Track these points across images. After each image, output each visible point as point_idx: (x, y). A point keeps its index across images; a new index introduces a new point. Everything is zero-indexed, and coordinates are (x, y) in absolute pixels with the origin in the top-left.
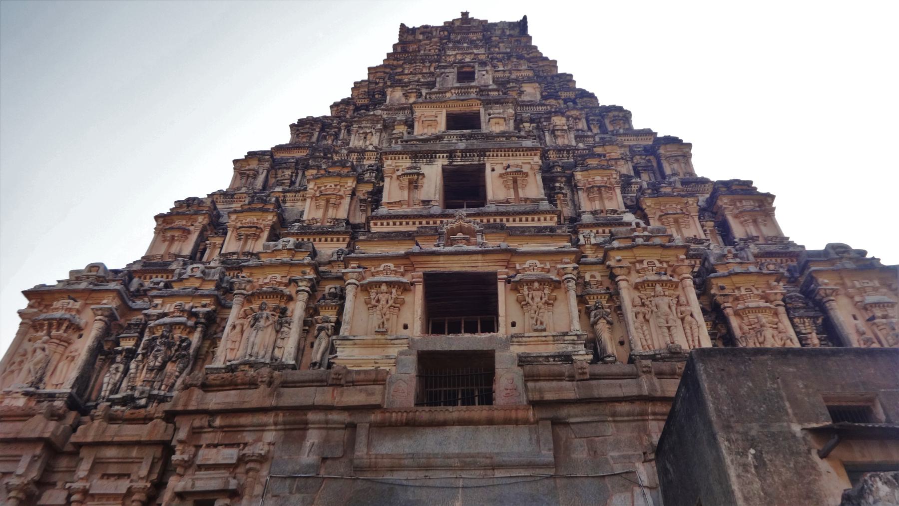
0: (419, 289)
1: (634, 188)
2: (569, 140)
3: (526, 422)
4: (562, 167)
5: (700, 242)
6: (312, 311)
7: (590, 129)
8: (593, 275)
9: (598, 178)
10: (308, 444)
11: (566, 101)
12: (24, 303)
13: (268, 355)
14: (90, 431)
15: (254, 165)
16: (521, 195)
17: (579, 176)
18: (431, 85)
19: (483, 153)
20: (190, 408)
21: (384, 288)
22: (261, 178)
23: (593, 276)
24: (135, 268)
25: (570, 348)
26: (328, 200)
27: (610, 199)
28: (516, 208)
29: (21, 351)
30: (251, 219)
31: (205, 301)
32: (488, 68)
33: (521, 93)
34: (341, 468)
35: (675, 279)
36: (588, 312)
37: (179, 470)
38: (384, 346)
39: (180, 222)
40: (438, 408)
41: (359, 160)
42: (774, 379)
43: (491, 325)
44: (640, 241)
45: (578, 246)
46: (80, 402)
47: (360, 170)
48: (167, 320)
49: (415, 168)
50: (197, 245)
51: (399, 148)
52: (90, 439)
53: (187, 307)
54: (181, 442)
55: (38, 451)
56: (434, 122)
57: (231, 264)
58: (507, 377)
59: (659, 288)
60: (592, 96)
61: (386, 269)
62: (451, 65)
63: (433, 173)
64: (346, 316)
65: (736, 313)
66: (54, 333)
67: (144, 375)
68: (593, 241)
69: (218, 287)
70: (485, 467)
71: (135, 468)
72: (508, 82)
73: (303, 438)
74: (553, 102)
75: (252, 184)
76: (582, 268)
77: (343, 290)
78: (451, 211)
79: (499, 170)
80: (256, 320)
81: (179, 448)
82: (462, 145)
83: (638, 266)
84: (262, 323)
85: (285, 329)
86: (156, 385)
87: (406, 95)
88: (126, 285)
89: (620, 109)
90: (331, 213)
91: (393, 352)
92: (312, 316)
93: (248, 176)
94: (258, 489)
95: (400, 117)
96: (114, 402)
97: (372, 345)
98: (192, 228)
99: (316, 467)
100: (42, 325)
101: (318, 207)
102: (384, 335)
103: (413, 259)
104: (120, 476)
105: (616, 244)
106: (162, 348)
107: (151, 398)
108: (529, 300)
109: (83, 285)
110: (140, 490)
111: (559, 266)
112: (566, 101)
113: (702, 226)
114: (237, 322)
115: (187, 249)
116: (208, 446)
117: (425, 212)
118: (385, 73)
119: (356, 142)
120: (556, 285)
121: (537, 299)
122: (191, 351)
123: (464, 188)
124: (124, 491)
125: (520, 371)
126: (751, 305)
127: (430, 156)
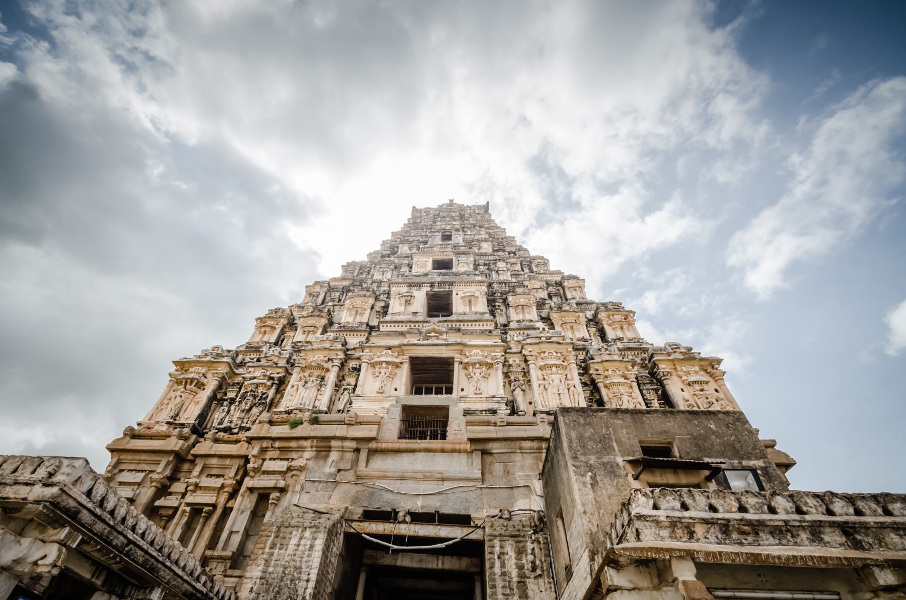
0: (406, 367)
1: (547, 306)
2: (506, 277)
3: (466, 451)
6: (341, 378)
7: (523, 270)
8: (515, 360)
9: (522, 300)
10: (330, 460)
11: (509, 253)
12: (173, 368)
13: (312, 404)
14: (204, 447)
15: (317, 289)
16: (473, 309)
17: (510, 299)
18: (426, 243)
19: (451, 284)
20: (261, 435)
21: (384, 365)
24: (241, 349)
25: (496, 406)
26: (357, 312)
27: (529, 313)
28: (469, 318)
29: (168, 397)
30: (312, 321)
31: (279, 370)
33: (480, 248)
34: (350, 476)
36: (510, 384)
37: (251, 474)
38: (382, 401)
39: (270, 322)
40: (414, 441)
41: (378, 287)
42: (607, 427)
44: (543, 339)
45: (506, 342)
46: (199, 430)
47: (378, 293)
48: (255, 381)
50: (279, 337)
51: (400, 280)
52: (202, 452)
53: (268, 373)
54: (254, 456)
55: (171, 458)
56: (424, 265)
57: (297, 349)
59: (554, 369)
60: (526, 250)
62: (438, 232)
64: (359, 383)
66: (188, 386)
67: (238, 414)
68: (516, 339)
69: (288, 362)
70: (438, 479)
71: (227, 471)
73: (327, 457)
74: (501, 253)
76: (507, 355)
77: (360, 366)
78: (429, 319)
79: (461, 294)
80: (306, 382)
81: (252, 460)
82: (439, 279)
83: (542, 355)
84: (309, 384)
85: (323, 389)
86: (245, 420)
87: (410, 249)
88: (234, 359)
89: (543, 258)
90: (358, 319)
91: (387, 405)
92: (340, 381)
94: (298, 488)
95: (406, 261)
96: (219, 430)
97: (374, 400)
99: (334, 475)
100: (181, 382)
101: (351, 315)
102: (382, 395)
103: (404, 348)
104: (218, 476)
105: (529, 341)
106: (251, 398)
108: (472, 374)
109: (208, 358)
110: (228, 486)
111: (493, 354)
112: (509, 253)
114: (295, 383)
115: (273, 339)
116: (270, 459)
117: (414, 319)
119: (377, 276)
120: (490, 366)
121: (478, 374)
122: (268, 401)
123: (439, 305)
124: (219, 485)
125: (464, 419)
127: (419, 285)
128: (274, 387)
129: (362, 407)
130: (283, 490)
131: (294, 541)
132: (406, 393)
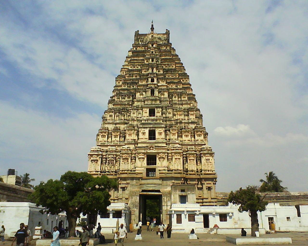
0: (146, 158)
4: (169, 126)
5: (189, 140)
6: (131, 160)
21: (141, 158)
22: (113, 116)
23: (170, 155)
32: (157, 90)
35: (180, 157)
39: (103, 133)
43: (156, 165)
49: (144, 131)
58: (157, 172)
59: (178, 159)
61: (141, 155)
63: (147, 131)
65: (189, 159)
66: (95, 161)
72: (161, 91)
75: (112, 118)
82: (152, 126)
83: (176, 155)
91: (143, 169)
93: (111, 116)
94: (129, 186)
98: (105, 134)
107: (111, 171)
113: (191, 135)
118: (132, 65)
123: (152, 135)
126: (191, 158)
127: (146, 128)
128: (115, 160)
129: (138, 170)
130: (126, 187)
131: (134, 198)
132: (147, 165)
